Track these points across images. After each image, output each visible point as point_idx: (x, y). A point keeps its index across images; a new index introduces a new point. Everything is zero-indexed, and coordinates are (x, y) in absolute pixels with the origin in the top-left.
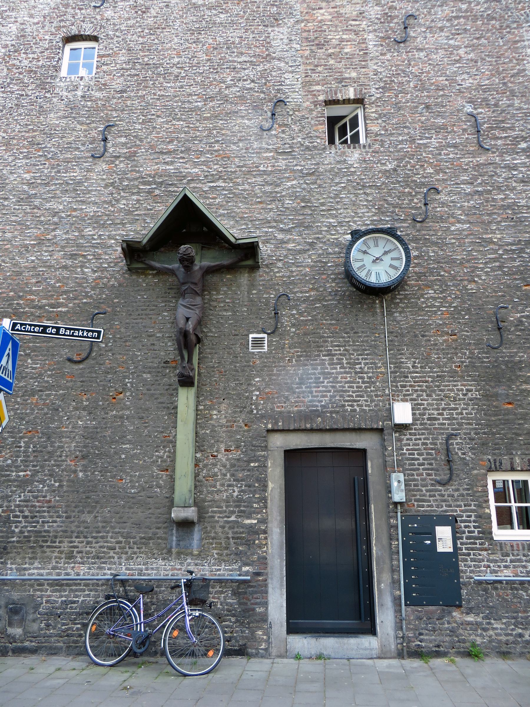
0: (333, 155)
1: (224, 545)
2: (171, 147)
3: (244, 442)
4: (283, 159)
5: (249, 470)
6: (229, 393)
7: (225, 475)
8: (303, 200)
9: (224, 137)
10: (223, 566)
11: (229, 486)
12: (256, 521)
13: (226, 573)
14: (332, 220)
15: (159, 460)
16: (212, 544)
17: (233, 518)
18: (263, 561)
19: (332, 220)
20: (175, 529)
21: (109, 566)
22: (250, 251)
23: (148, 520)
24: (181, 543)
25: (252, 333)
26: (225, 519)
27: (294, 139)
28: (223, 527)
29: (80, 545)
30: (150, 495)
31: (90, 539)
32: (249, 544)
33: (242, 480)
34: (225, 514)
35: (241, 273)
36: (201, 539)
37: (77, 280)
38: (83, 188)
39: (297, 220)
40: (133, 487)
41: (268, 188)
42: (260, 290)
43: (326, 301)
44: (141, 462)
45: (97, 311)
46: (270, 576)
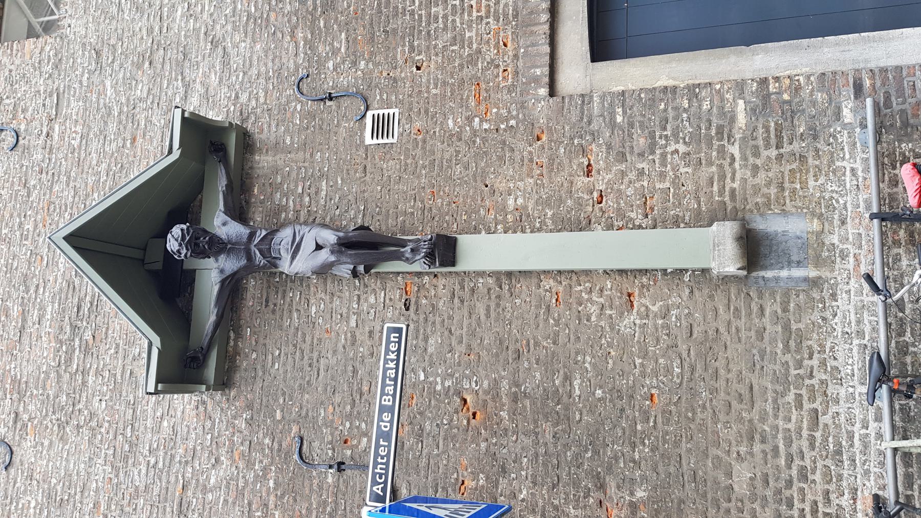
0: (74, 21)
1: (794, 166)
2: (15, 311)
3: (572, 139)
4: (68, 106)
5: (631, 125)
6: (474, 176)
7: (641, 173)
8: (139, 66)
9: (15, 214)
10: (845, 164)
11: (664, 163)
12: (741, 103)
13: (860, 155)
14: (179, 13)
15: (608, 312)
16: (794, 191)
17: (735, 150)
18: (827, 80)
19: (179, 13)
20: (762, 273)
21: (858, 425)
22: (206, 141)
23: (743, 334)
24: (795, 258)
25: (363, 141)
27: (39, 91)
28: (755, 169)
29: (809, 497)
30: (685, 333)
31: (794, 472)
32: (791, 112)
33: (653, 137)
34: (727, 167)
35: (251, 168)
36: (784, 213)
37: (230, 500)
38: (59, 488)
39: (170, 73)
40: (668, 371)
41: (112, 127)
42: (287, 130)
43: (315, 8)
44: (613, 353)
45: (296, 457)
46: (862, 66)
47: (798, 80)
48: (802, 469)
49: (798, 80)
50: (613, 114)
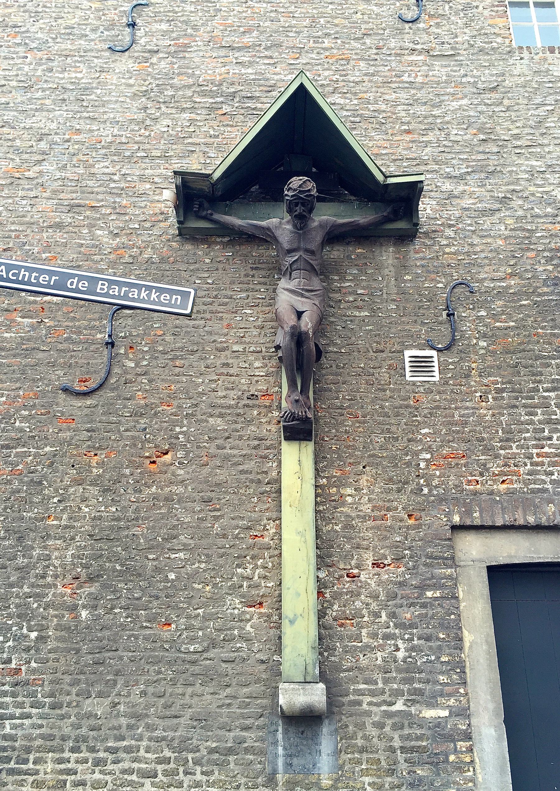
1: (383, 763)
11: (386, 637)
17: (399, 706)
20: (280, 729)
23: (225, 710)
26: (384, 708)
28: (380, 726)
31: (101, 755)
34: (382, 698)
47: (469, 770)
48: (104, 762)
49: (469, 770)
50: (434, 587)
